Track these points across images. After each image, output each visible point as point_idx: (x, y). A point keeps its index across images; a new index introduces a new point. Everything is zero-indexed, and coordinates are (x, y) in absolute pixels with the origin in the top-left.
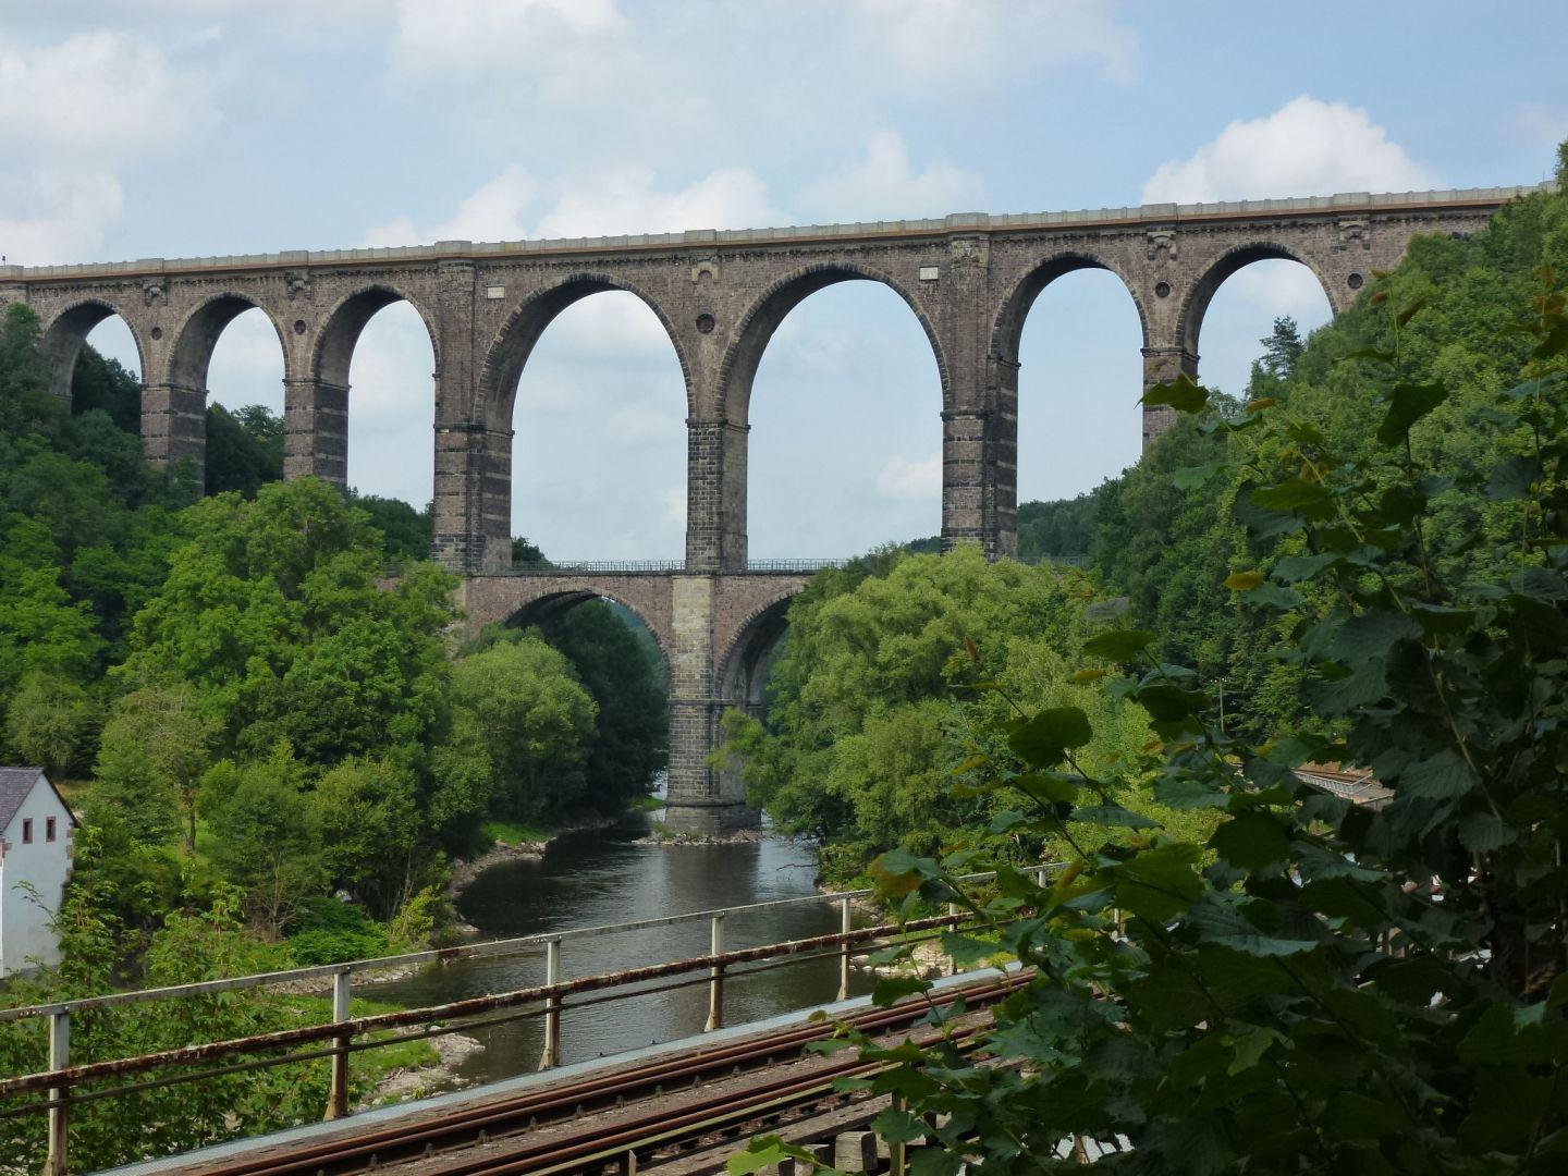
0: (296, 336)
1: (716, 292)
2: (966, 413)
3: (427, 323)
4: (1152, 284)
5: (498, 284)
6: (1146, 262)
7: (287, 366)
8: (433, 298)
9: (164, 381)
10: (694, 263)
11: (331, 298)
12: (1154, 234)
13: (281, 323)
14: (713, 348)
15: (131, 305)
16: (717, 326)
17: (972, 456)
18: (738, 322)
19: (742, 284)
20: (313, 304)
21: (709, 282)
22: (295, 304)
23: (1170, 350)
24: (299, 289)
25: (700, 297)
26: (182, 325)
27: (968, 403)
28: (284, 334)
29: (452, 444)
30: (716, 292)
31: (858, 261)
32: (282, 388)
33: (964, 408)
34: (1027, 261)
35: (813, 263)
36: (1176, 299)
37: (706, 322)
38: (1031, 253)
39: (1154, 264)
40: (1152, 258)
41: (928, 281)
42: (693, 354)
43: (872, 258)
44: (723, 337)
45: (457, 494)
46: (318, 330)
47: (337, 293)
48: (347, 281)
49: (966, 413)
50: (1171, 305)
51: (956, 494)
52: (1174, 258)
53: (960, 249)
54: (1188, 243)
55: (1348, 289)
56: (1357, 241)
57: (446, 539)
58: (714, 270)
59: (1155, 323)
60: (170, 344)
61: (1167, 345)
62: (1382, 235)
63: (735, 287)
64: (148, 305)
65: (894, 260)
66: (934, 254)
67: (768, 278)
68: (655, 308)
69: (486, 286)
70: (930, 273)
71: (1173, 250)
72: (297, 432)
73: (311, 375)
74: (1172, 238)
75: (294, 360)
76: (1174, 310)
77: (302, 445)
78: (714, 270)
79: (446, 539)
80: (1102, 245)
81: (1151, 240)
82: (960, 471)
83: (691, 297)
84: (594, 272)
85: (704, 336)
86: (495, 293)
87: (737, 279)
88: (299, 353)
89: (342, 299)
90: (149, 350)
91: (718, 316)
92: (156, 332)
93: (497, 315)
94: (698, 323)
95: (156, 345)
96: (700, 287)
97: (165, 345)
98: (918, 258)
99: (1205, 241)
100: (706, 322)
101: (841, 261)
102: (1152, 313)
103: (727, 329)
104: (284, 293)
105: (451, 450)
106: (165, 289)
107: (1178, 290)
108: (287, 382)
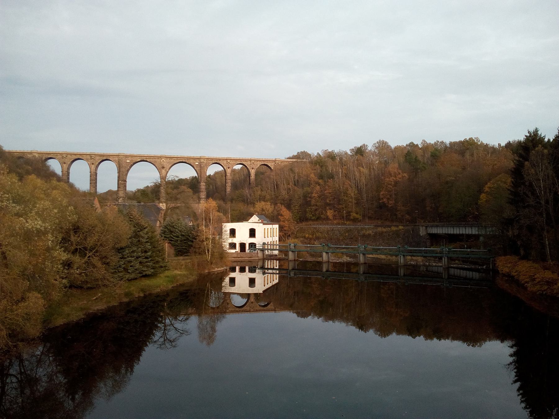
0: (92, 165)
1: (165, 164)
5: (129, 160)
8: (117, 161)
10: (161, 159)
11: (98, 159)
13: (89, 163)
14: (164, 171)
16: (165, 169)
19: (169, 163)
24: (92, 158)
25: (162, 164)
26: (70, 162)
29: (122, 183)
32: (89, 173)
35: (180, 161)
37: (163, 167)
38: (211, 162)
43: (189, 161)
44: (166, 170)
47: (99, 159)
52: (230, 164)
53: (202, 160)
57: (120, 197)
58: (164, 160)
64: (63, 158)
70: (197, 163)
78: (164, 160)
79: (120, 197)
80: (221, 162)
81: (227, 161)
85: (163, 170)
89: (101, 160)
92: (65, 163)
95: (65, 165)
98: (195, 161)
99: (234, 162)
100: (163, 167)
101: (184, 161)
108: (90, 172)
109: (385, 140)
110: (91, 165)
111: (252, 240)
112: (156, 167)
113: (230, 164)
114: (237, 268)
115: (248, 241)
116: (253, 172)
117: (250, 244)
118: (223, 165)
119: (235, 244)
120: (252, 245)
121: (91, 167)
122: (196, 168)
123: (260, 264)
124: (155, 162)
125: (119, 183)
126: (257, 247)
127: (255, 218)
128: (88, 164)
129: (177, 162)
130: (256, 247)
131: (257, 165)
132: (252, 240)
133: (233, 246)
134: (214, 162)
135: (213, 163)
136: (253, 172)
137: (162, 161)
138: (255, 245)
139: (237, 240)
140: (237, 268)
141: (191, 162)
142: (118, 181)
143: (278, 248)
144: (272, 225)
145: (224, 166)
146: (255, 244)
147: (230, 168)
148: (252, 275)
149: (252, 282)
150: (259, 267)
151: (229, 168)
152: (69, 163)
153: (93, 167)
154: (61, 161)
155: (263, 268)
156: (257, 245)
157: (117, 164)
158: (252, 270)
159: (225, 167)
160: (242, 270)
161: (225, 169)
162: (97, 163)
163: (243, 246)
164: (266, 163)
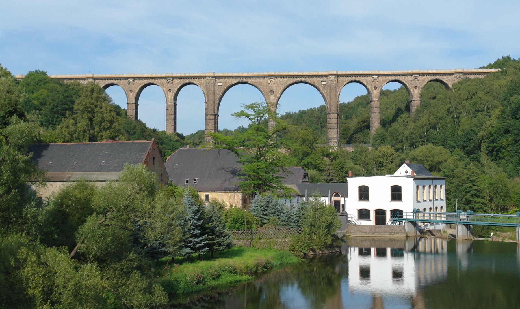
0: (169, 93)
1: (274, 85)
2: (334, 113)
3: (203, 90)
4: (373, 87)
6: (372, 82)
7: (166, 100)
9: (133, 102)
11: (178, 83)
12: (374, 76)
13: (164, 89)
14: (273, 98)
15: (124, 84)
17: (335, 122)
18: (279, 92)
19: (280, 84)
20: (173, 85)
21: (272, 83)
22: (168, 85)
23: (377, 101)
25: (270, 86)
27: (334, 111)
28: (166, 92)
30: (274, 85)
31: (307, 79)
33: (333, 112)
34: (346, 81)
36: (378, 90)
37: (272, 92)
39: (373, 82)
40: (373, 81)
41: (323, 85)
42: (269, 99)
44: (275, 96)
45: (212, 129)
46: (175, 92)
48: (182, 80)
49: (334, 113)
50: (377, 91)
51: (332, 130)
52: (378, 81)
53: (331, 78)
54: (380, 78)
55: (414, 89)
56: (416, 79)
59: (374, 95)
60: (135, 94)
61: (376, 100)
62: (421, 78)
63: (278, 84)
64: (129, 84)
65: (315, 80)
66: (325, 78)
67: (286, 83)
68: (259, 89)
69: (218, 82)
70: (324, 83)
71: (378, 80)
72: (169, 115)
73: (173, 102)
74: (378, 77)
75: (168, 98)
76: (378, 92)
77: (171, 118)
78: (274, 81)
82: (332, 126)
83: (268, 86)
84: (244, 80)
86: (220, 84)
87: (279, 83)
88: (169, 96)
90: (129, 95)
91: (274, 91)
92: (131, 91)
93: (220, 89)
94: (270, 92)
95: (131, 94)
96: (270, 84)
97: (133, 94)
99: (384, 78)
100: (272, 92)
101: (303, 79)
102: (373, 93)
103: (277, 94)
104: (165, 82)
105: (210, 119)
106: (134, 81)
107: (379, 88)
109: (41, 68)
110: (167, 92)
111: (396, 205)
112: (261, 92)
113: (378, 81)
114: (373, 250)
115: (389, 206)
116: (416, 94)
117: (392, 211)
118: (365, 84)
119: (369, 211)
120: (397, 214)
121: (168, 95)
122: (322, 91)
123: (409, 245)
124: (260, 83)
125: (208, 118)
126: (404, 217)
127: (404, 169)
128: (163, 90)
129: (292, 82)
130: (402, 217)
131: (423, 81)
132: (396, 205)
133: (364, 214)
134: (350, 79)
135: (350, 80)
136: (416, 94)
137: (269, 81)
138: (402, 214)
139: (371, 205)
140: (373, 250)
141: (315, 80)
142: (206, 115)
143: (444, 219)
144: (431, 181)
145: (367, 85)
146: (402, 211)
147: (377, 89)
148: (397, 262)
149: (397, 275)
150: (407, 249)
151: (375, 88)
152: (137, 90)
153: (171, 96)
154: (126, 88)
155: (414, 250)
156: (404, 214)
157: (204, 89)
158: (398, 253)
159: (369, 87)
160: (381, 253)
161: (370, 89)
162: (176, 89)
163: (380, 214)
164: (438, 77)
